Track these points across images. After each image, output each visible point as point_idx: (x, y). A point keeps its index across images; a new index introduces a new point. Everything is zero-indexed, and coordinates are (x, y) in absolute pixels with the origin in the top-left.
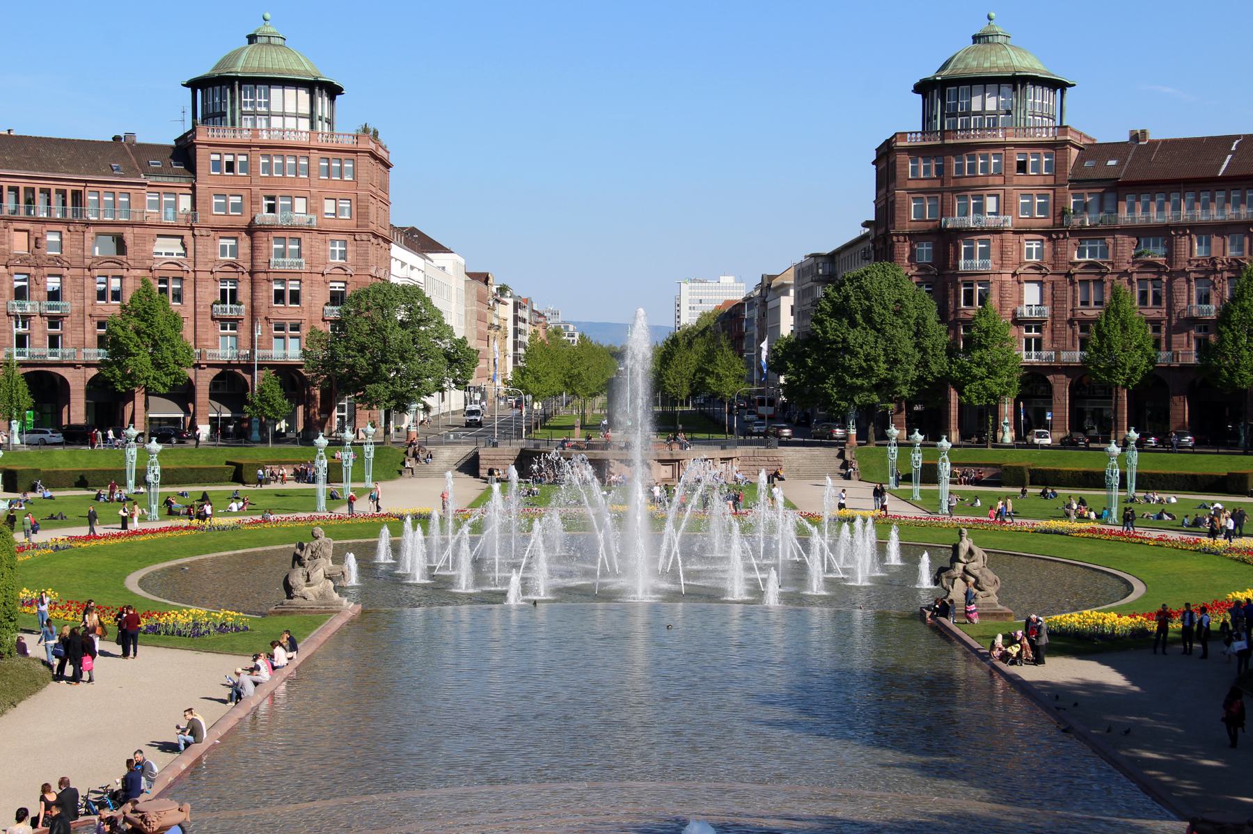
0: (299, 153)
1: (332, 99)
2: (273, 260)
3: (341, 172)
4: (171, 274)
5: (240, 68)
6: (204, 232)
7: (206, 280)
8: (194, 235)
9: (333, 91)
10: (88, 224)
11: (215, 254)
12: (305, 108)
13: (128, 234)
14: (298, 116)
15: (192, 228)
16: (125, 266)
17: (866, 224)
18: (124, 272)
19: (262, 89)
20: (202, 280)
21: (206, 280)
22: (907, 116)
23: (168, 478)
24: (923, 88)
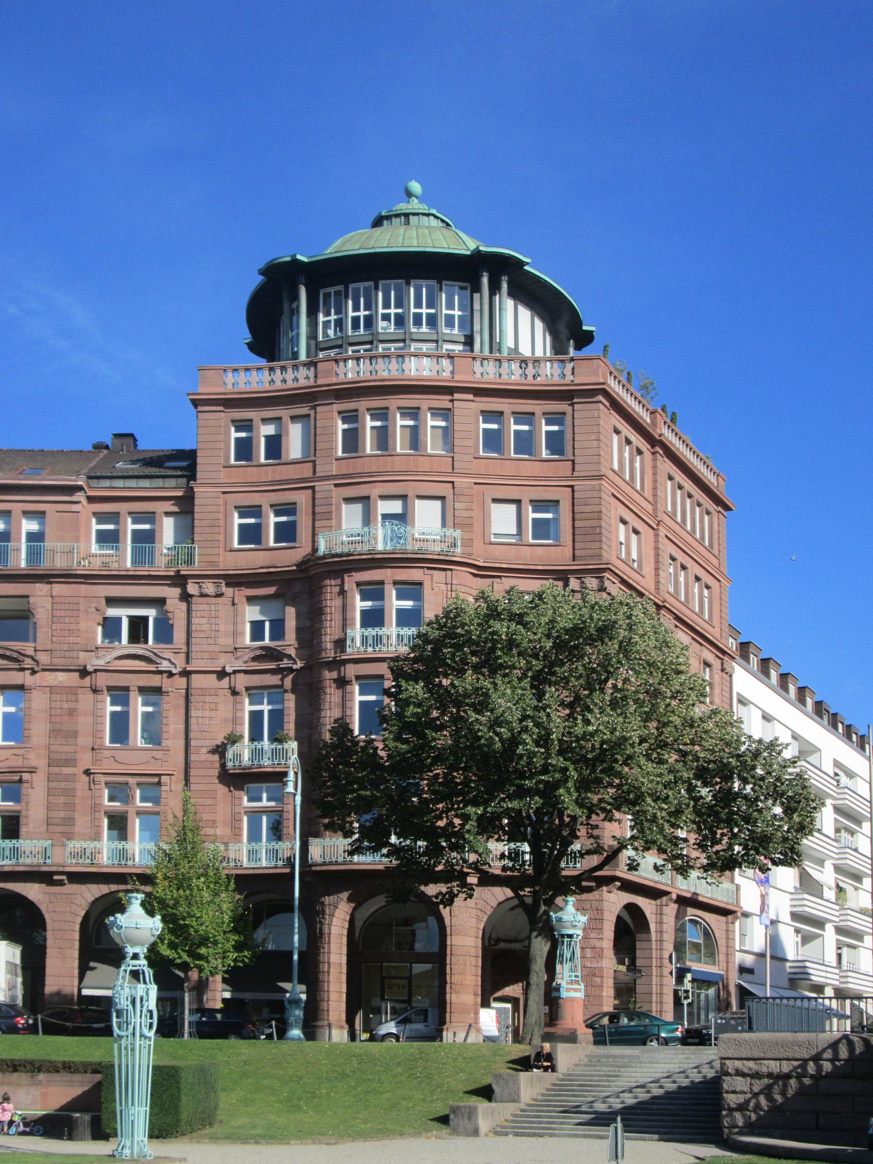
0: (425, 402)
2: (356, 632)
3: (525, 443)
4: (134, 681)
6: (209, 588)
7: (215, 692)
8: (186, 597)
11: (236, 634)
15: (179, 580)
16: (28, 663)
18: (26, 678)
20: (204, 692)
21: (215, 692)
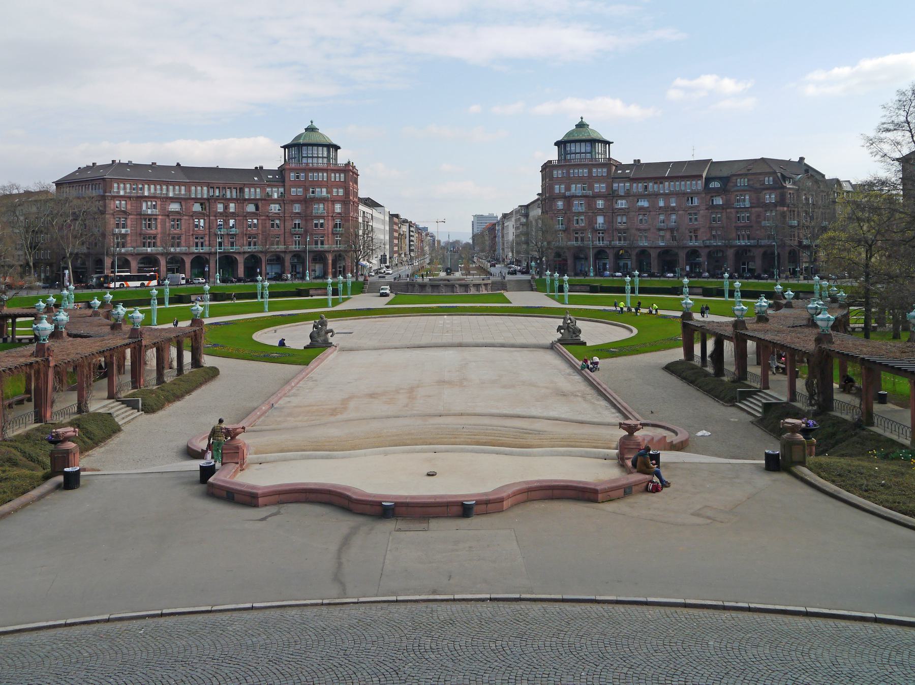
1: (336, 151)
5: (301, 141)
9: (337, 148)
10: (245, 200)
12: (325, 155)
13: (260, 205)
14: (323, 157)
17: (538, 194)
19: (310, 148)
22: (553, 155)
23: (272, 295)
24: (558, 144)
